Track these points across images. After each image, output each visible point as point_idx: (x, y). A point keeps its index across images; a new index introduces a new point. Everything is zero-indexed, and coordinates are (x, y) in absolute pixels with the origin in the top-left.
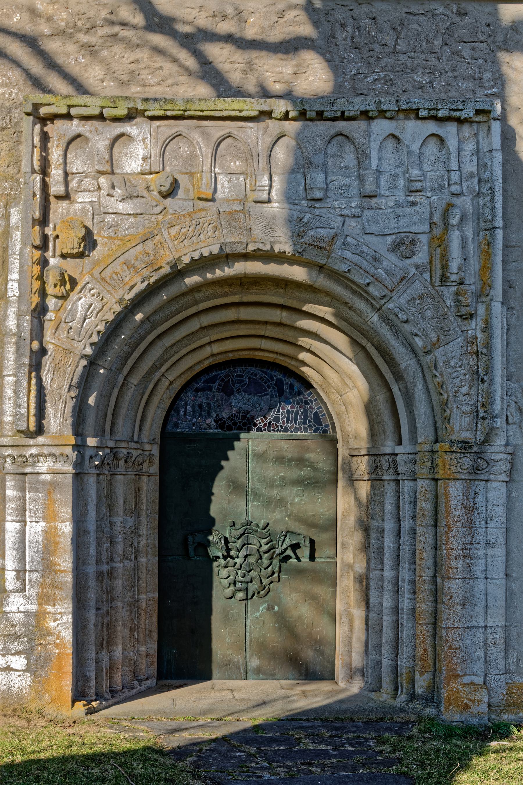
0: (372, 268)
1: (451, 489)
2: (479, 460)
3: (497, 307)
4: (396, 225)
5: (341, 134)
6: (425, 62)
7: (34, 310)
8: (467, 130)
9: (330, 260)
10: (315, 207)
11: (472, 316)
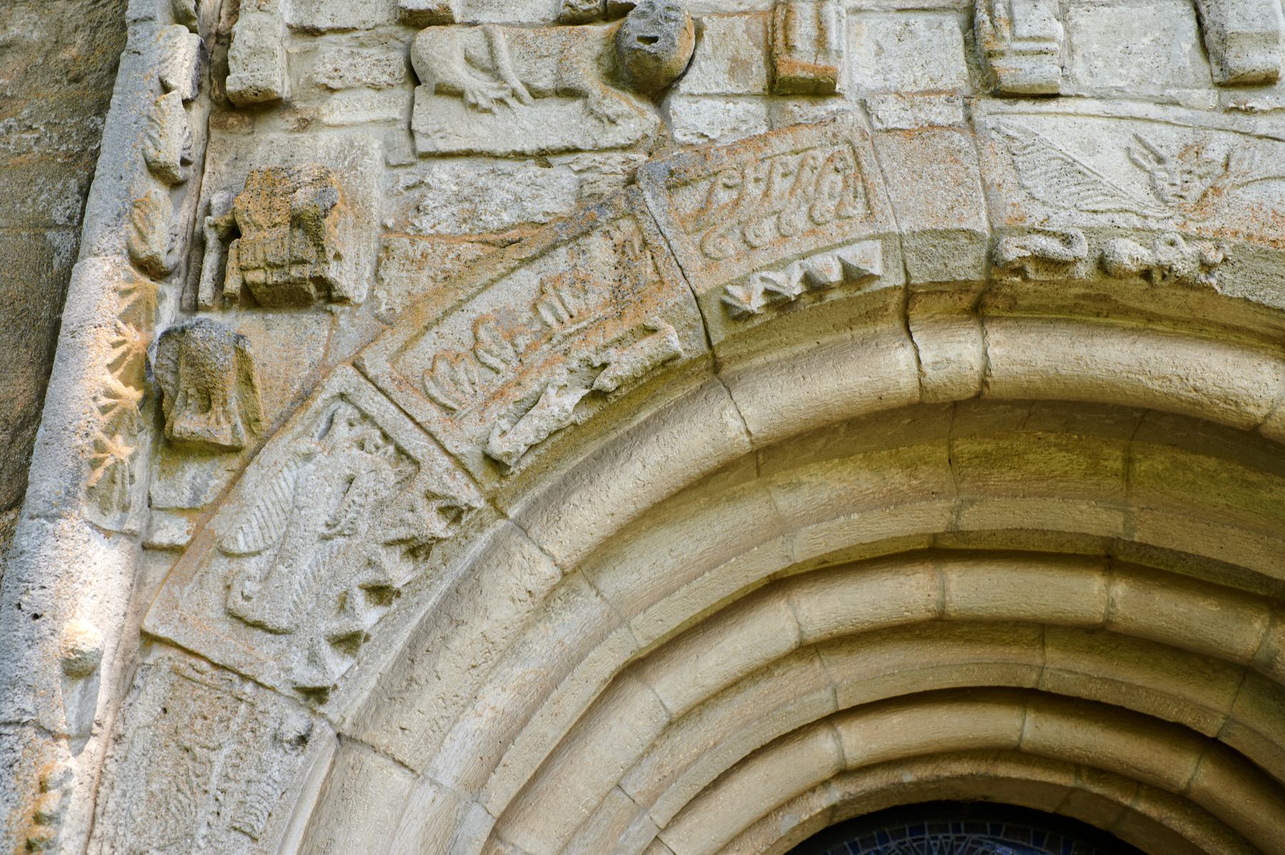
10: (1250, 111)
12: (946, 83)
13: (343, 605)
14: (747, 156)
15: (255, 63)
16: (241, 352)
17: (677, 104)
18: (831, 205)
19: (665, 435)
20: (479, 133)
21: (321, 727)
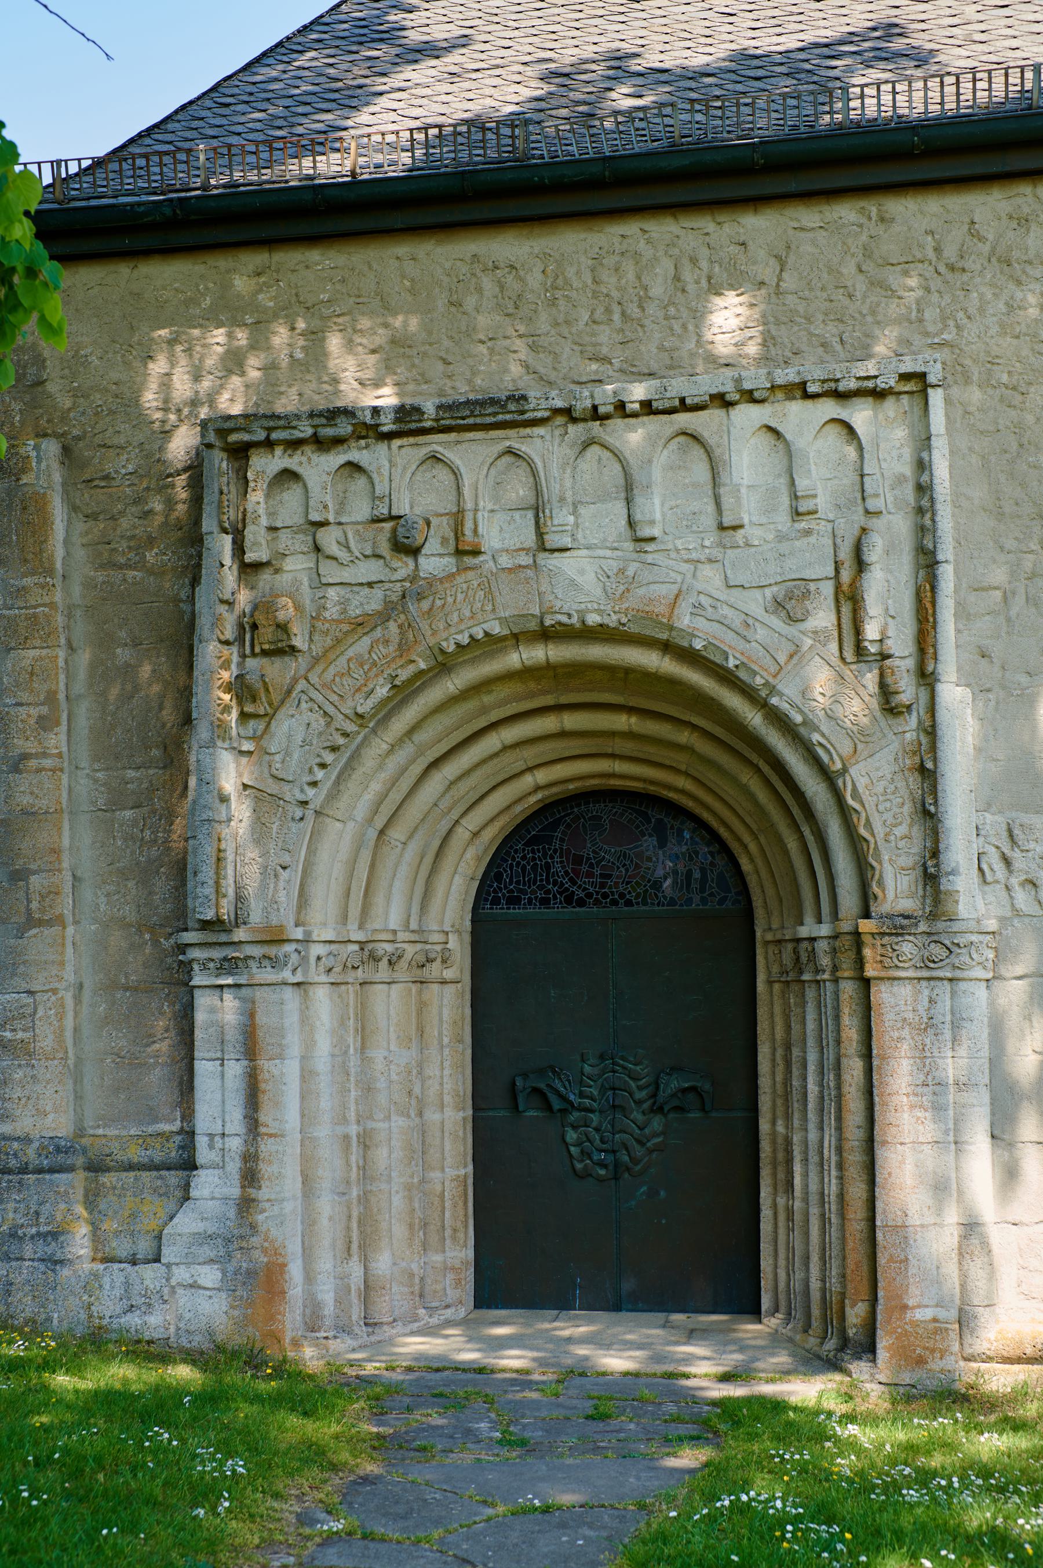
0: (742, 641)
1: (884, 995)
2: (933, 945)
4: (779, 570)
5: (685, 434)
6: (827, 304)
9: (674, 633)
12: (526, 545)
13: (311, 771)
14: (447, 585)
15: (255, 548)
16: (264, 682)
17: (421, 560)
18: (479, 605)
19: (426, 693)
20: (346, 575)
21: (307, 812)
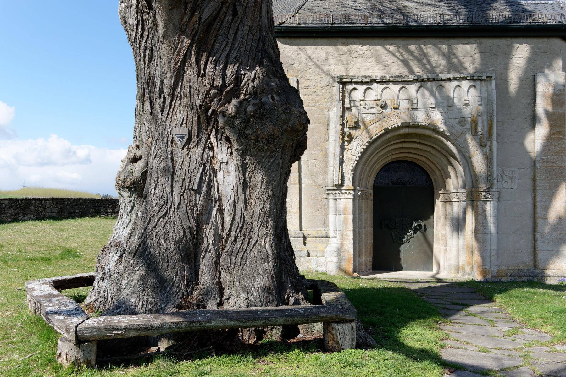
3: (494, 143)
7: (340, 146)
8: (483, 83)
11: (485, 146)
